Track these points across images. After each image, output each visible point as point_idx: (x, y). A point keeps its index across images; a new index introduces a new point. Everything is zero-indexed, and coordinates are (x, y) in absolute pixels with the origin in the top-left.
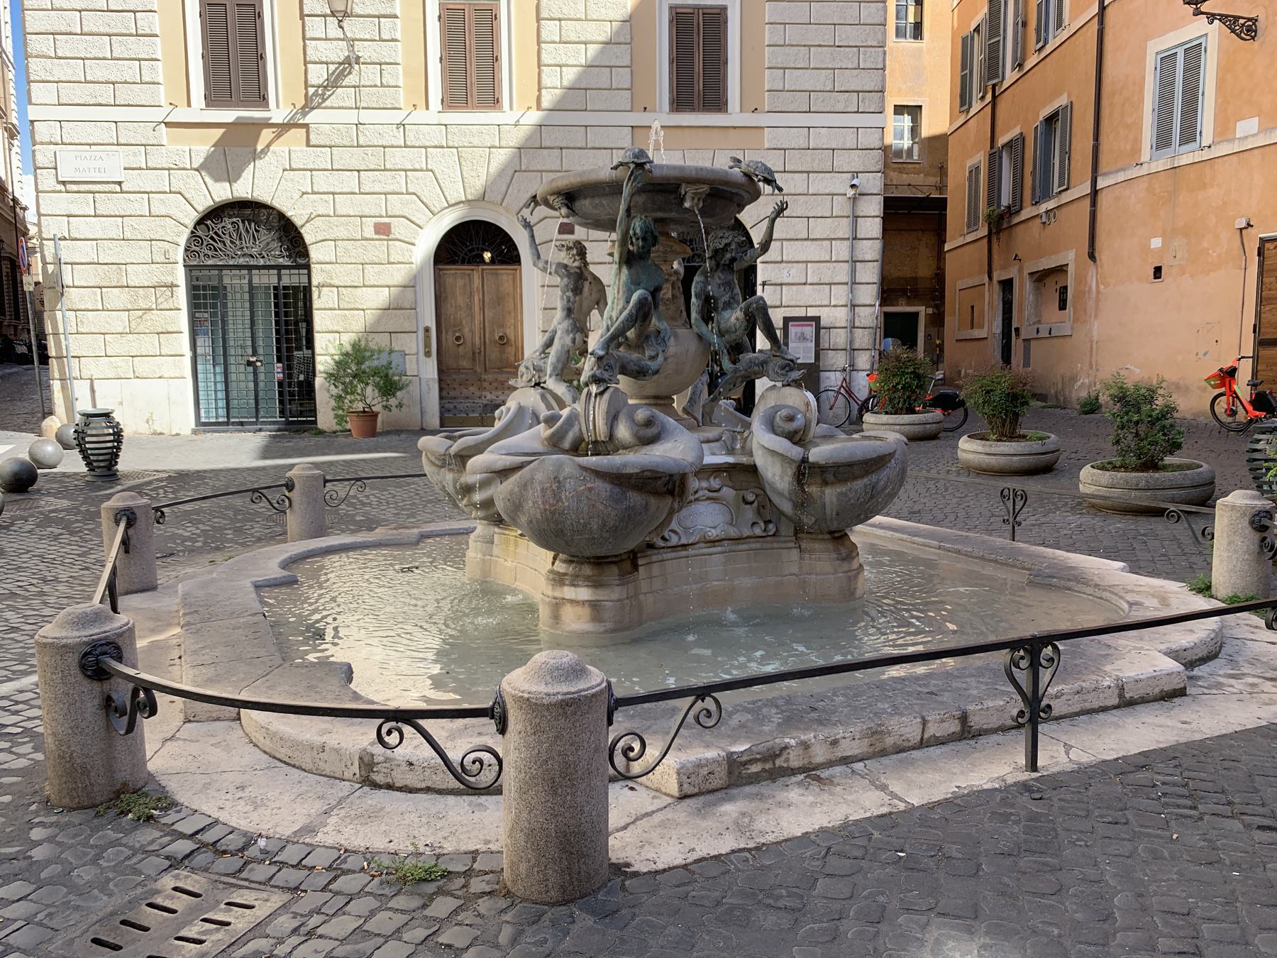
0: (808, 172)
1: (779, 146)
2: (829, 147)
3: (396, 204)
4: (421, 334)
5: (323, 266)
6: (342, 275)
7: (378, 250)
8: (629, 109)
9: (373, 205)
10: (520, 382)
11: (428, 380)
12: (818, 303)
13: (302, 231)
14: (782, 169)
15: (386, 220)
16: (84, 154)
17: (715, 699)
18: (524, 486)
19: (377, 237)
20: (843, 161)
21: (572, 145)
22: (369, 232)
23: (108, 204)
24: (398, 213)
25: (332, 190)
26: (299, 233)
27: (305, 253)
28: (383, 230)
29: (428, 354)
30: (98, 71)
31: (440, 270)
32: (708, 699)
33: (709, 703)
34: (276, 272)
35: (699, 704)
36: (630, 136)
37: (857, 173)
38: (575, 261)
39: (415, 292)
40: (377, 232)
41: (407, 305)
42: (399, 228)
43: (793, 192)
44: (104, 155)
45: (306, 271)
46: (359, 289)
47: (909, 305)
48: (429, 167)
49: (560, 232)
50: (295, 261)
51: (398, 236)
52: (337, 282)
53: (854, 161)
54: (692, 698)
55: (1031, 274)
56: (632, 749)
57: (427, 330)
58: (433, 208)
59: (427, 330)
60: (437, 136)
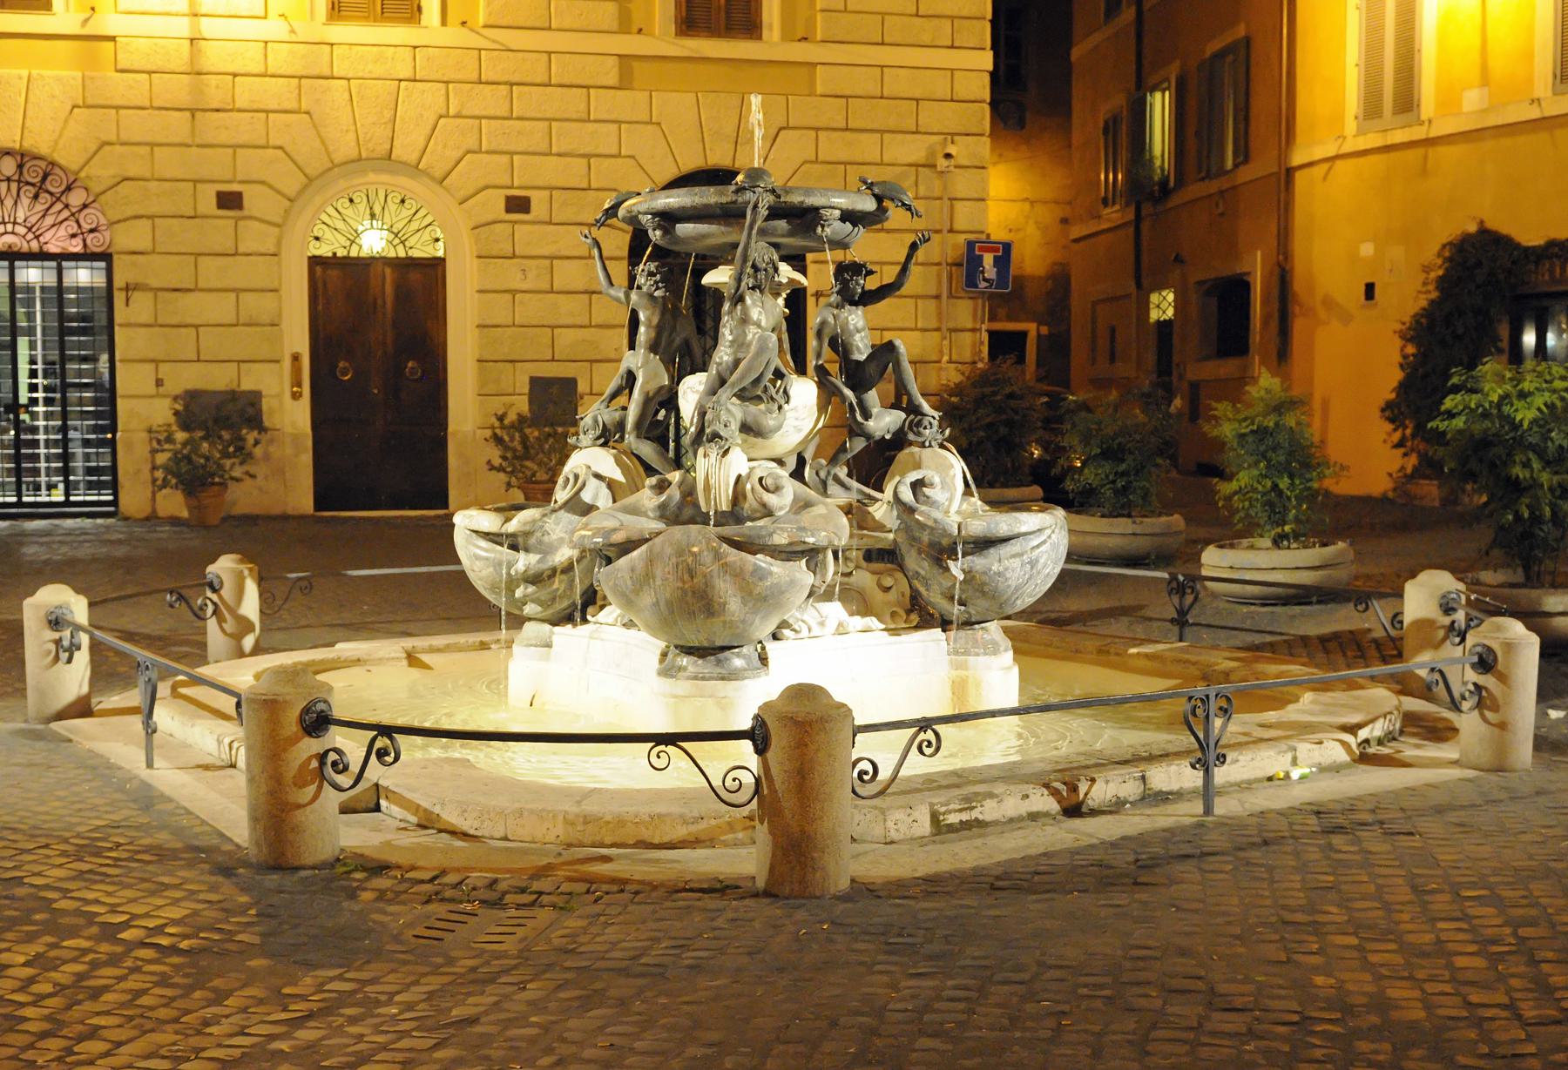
0: (882, 132)
1: (839, 93)
2: (910, 96)
3: (251, 164)
4: (287, 363)
5: (134, 257)
6: (160, 272)
8: (615, 26)
10: (585, 440)
12: (900, 324)
14: (843, 125)
15: (235, 187)
17: (937, 734)
18: (650, 561)
20: (933, 117)
21: (528, 80)
22: (208, 203)
24: (255, 177)
28: (230, 201)
29: (296, 396)
32: (929, 731)
33: (930, 735)
34: (54, 264)
35: (922, 736)
36: (615, 71)
37: (953, 134)
38: (658, 288)
41: (265, 319)
42: (255, 200)
43: (860, 160)
45: (103, 264)
47: (1010, 319)
49: (508, 210)
51: (258, 215)
52: (154, 283)
53: (950, 118)
54: (914, 730)
55: (1200, 283)
56: (866, 773)
57: (296, 358)
58: (308, 171)
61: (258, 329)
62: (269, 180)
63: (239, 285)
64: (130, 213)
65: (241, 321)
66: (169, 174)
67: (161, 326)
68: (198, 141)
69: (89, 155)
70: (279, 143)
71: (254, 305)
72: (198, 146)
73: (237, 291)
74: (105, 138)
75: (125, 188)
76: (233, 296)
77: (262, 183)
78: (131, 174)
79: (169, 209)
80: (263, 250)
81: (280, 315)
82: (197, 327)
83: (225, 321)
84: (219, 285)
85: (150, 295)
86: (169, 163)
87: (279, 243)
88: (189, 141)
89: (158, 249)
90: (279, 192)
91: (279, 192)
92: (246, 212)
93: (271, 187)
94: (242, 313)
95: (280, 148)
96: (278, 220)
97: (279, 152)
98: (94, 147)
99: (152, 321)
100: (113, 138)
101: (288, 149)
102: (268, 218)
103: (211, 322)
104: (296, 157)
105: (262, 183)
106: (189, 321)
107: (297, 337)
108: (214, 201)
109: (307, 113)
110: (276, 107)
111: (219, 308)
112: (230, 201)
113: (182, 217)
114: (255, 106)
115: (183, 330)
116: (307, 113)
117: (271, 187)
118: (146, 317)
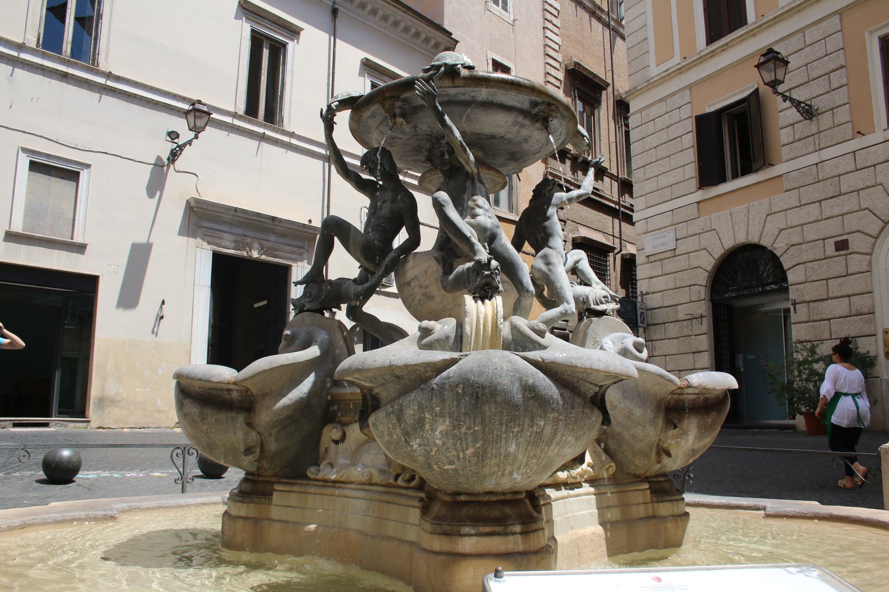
3: (852, 222)
5: (797, 286)
7: (836, 266)
9: (832, 228)
13: (781, 259)
16: (658, 236)
19: (838, 253)
22: (830, 249)
23: (670, 266)
24: (854, 229)
25: (800, 222)
26: (780, 263)
27: (785, 279)
30: (664, 181)
39: (873, 297)
40: (837, 250)
41: (864, 310)
42: (857, 243)
44: (666, 234)
46: (826, 302)
48: (879, 181)
50: (781, 286)
51: (856, 250)
52: (807, 298)
58: (883, 218)
61: (861, 317)
62: (862, 229)
63: (850, 293)
64: (794, 263)
65: (853, 313)
66: (811, 239)
67: (813, 321)
68: (824, 217)
69: (775, 237)
70: (865, 206)
71: (858, 302)
72: (825, 219)
73: (849, 296)
74: (781, 227)
75: (792, 251)
76: (847, 298)
77: (859, 231)
78: (793, 243)
79: (812, 257)
80: (861, 270)
81: (874, 307)
82: (829, 320)
83: (844, 315)
84: (839, 294)
85: (806, 304)
86: (811, 233)
87: (870, 263)
88: (820, 218)
89: (808, 280)
92: (850, 251)
93: (863, 233)
94: (853, 309)
95: (867, 209)
96: (869, 251)
97: (867, 212)
98: (777, 233)
99: (807, 319)
100: (784, 226)
101: (870, 208)
102: (862, 251)
103: (837, 316)
104: (875, 212)
105: (859, 231)
106: (825, 317)
108: (834, 247)
109: (881, 184)
110: (862, 186)
111: (839, 307)
112: (842, 246)
113: (819, 260)
114: (851, 189)
115: (823, 322)
116: (881, 184)
117: (863, 233)
118: (804, 319)
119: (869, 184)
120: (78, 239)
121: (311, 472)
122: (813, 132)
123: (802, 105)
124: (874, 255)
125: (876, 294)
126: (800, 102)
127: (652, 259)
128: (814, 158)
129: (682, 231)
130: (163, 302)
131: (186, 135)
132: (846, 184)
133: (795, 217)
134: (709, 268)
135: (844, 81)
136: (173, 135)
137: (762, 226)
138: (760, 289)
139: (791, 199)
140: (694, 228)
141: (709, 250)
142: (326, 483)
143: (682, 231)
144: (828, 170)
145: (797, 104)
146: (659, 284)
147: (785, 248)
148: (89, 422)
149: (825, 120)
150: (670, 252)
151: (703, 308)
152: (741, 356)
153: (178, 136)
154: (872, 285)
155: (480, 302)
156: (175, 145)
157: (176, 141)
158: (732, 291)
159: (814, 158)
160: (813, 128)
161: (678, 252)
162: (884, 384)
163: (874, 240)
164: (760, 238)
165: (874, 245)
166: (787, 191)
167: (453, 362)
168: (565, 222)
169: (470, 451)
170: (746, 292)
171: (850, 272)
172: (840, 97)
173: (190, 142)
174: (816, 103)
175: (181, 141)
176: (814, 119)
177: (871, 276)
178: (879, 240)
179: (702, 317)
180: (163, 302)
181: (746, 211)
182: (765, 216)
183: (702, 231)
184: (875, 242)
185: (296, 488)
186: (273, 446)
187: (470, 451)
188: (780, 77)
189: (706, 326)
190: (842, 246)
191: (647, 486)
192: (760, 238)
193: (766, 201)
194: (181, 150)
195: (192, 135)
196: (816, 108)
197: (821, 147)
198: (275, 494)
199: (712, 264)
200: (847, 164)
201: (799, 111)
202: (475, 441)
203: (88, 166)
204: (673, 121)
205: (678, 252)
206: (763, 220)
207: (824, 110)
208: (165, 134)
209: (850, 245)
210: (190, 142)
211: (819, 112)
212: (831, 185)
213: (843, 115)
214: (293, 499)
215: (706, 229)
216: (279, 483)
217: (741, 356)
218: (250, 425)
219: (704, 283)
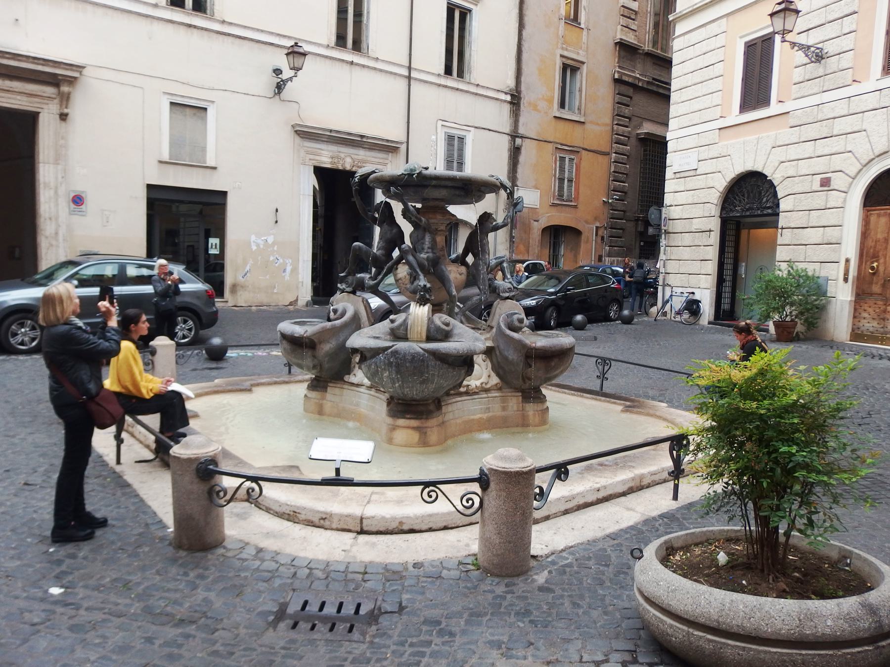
3: (837, 162)
7: (818, 200)
9: (819, 165)
11: (842, 301)
22: (816, 186)
23: (692, 183)
24: (837, 169)
27: (778, 205)
28: (825, 183)
29: (846, 280)
31: (868, 211)
40: (822, 185)
41: (834, 241)
42: (838, 181)
48: (864, 128)
57: (847, 261)
59: (847, 261)
60: (872, 101)
62: (843, 169)
66: (802, 174)
75: (785, 183)
78: (789, 175)
81: (841, 238)
86: (804, 167)
87: (845, 200)
90: (847, 175)
91: (847, 175)
107: (850, 249)
108: (819, 183)
119: (855, 129)
120: (210, 162)
121: (346, 378)
122: (821, 74)
123: (812, 49)
124: (849, 194)
125: (845, 228)
126: (809, 47)
127: (678, 175)
128: (816, 100)
129: (705, 153)
130: (277, 210)
131: (287, 73)
132: (840, 126)
133: (794, 152)
134: (721, 189)
135: (853, 27)
136: (278, 72)
137: (766, 157)
138: (759, 212)
139: (793, 135)
140: (714, 151)
141: (723, 173)
142: (352, 384)
143: (705, 153)
144: (827, 111)
145: (805, 48)
146: (681, 198)
147: (782, 179)
148: (227, 302)
149: (832, 64)
150: (693, 172)
151: (715, 224)
152: (744, 264)
153: (281, 72)
154: (843, 220)
155: (418, 307)
156: (280, 80)
157: (280, 76)
158: (738, 211)
159: (816, 100)
160: (821, 72)
161: (698, 172)
162: (838, 303)
163: (851, 180)
164: (764, 167)
165: (851, 184)
166: (791, 127)
167: (393, 346)
168: (630, 119)
169: (397, 385)
170: (748, 213)
171: (828, 206)
172: (846, 43)
173: (291, 79)
174: (829, 48)
175: (284, 76)
176: (823, 61)
177: (843, 212)
178: (855, 181)
179: (710, 231)
180: (277, 210)
181: (755, 142)
182: (770, 148)
183: (719, 156)
184: (852, 182)
185: (339, 385)
186: (326, 366)
187: (397, 385)
188: (788, 27)
189: (714, 238)
190: (825, 183)
191: (520, 394)
192: (764, 167)
193: (772, 133)
194: (285, 85)
195: (292, 73)
196: (826, 51)
197: (825, 89)
198: (329, 388)
199: (724, 186)
200: (841, 108)
201: (807, 56)
202: (398, 382)
203: (213, 102)
204: (709, 49)
205: (698, 172)
206: (768, 152)
207: (832, 54)
208: (271, 71)
209: (832, 182)
210: (291, 79)
211: (828, 55)
212: (826, 126)
213: (846, 60)
214: (337, 391)
215: (723, 155)
216: (331, 382)
217: (744, 264)
218: (314, 357)
219: (715, 202)
